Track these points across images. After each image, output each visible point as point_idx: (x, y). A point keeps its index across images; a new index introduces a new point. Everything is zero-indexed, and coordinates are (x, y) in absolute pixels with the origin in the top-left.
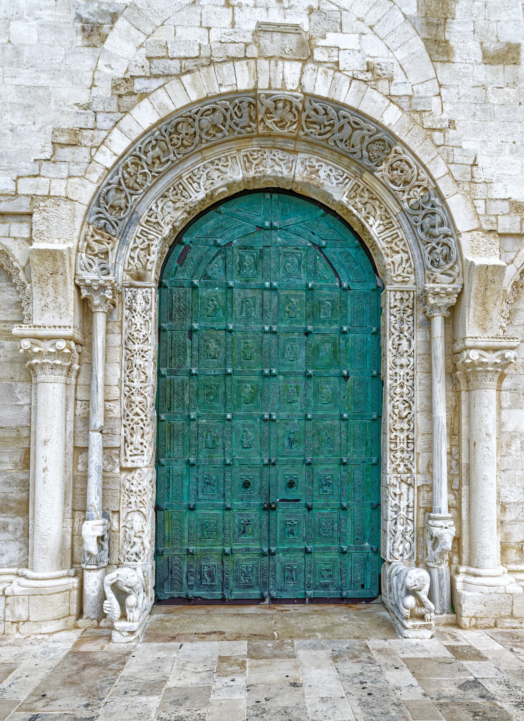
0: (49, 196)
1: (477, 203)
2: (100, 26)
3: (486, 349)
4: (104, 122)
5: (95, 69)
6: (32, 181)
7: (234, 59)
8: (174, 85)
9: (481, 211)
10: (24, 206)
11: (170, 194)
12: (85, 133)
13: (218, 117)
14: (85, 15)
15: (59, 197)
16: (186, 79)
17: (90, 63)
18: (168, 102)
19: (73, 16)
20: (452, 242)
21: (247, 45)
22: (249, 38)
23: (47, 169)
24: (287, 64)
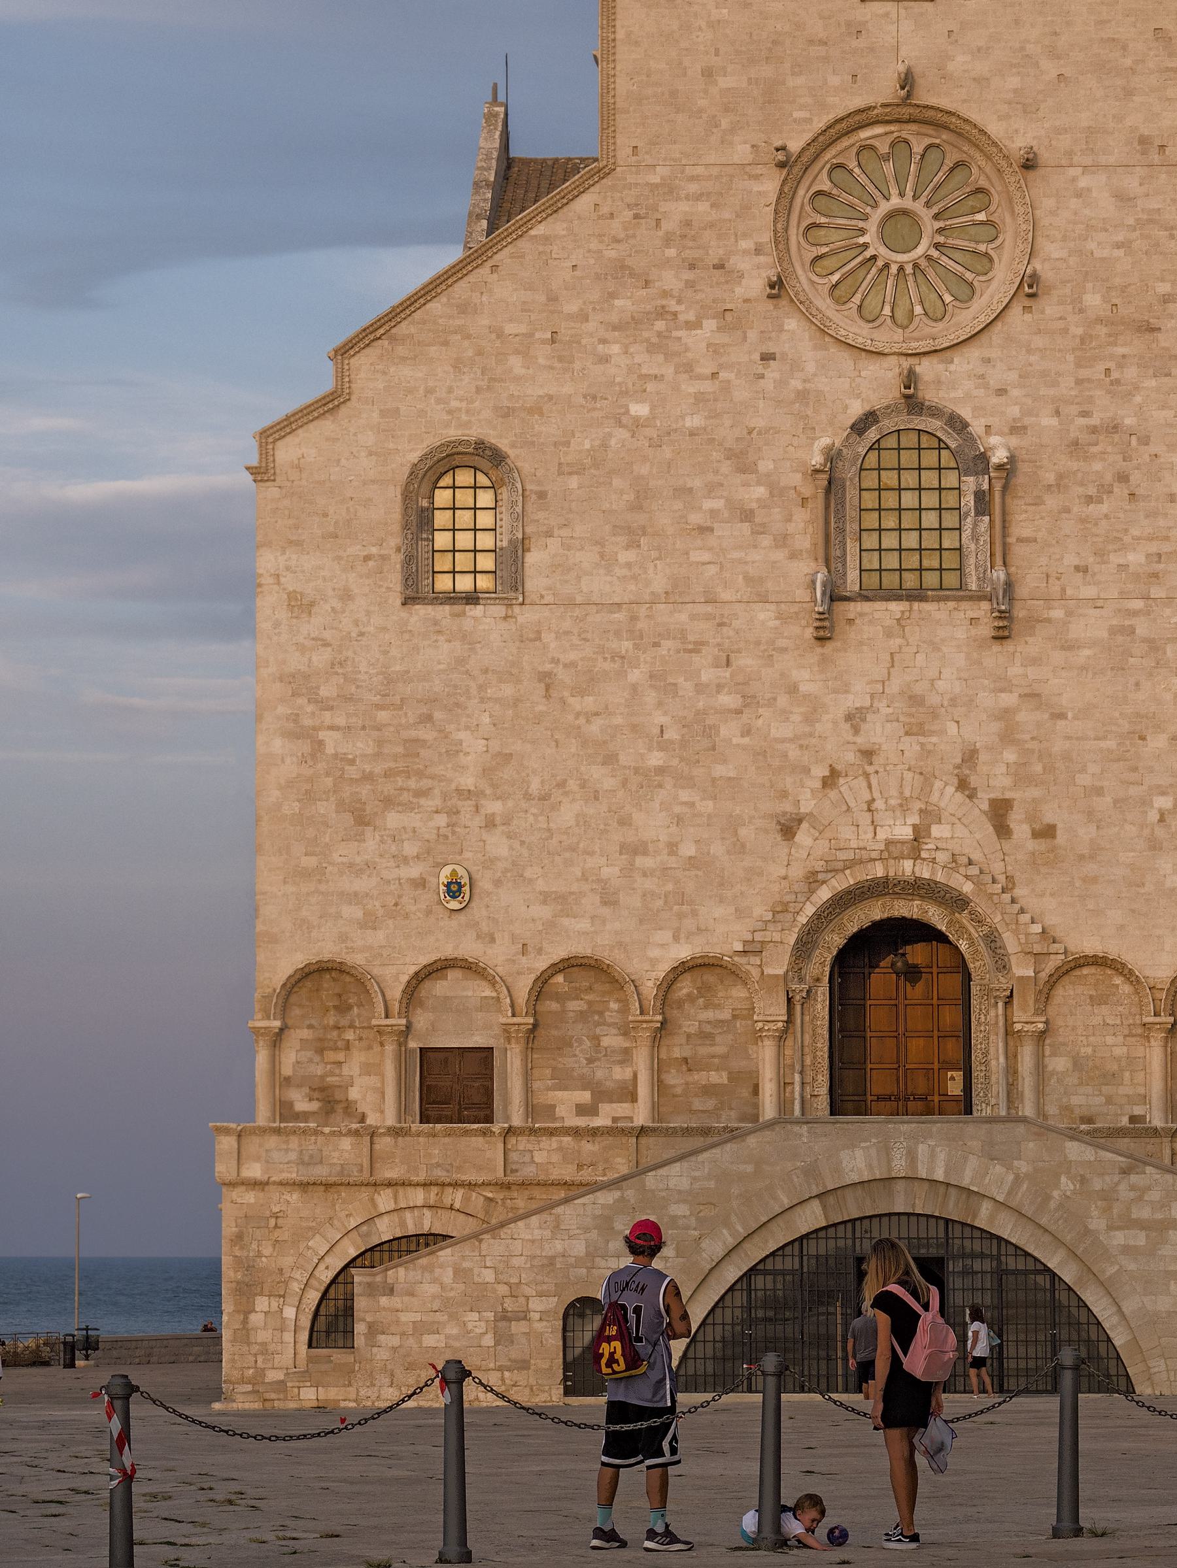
0: (771, 941)
1: (1020, 936)
2: (791, 828)
3: (1027, 1023)
4: (801, 898)
5: (790, 854)
6: (762, 933)
7: (875, 860)
8: (840, 876)
9: (1023, 941)
10: (758, 947)
11: (836, 929)
12: (791, 905)
13: (865, 889)
14: (783, 821)
15: (777, 942)
16: (848, 872)
17: (786, 850)
18: (837, 885)
19: (775, 822)
20: (1006, 959)
21: (882, 851)
22: (883, 848)
23: (771, 927)
24: (905, 861)
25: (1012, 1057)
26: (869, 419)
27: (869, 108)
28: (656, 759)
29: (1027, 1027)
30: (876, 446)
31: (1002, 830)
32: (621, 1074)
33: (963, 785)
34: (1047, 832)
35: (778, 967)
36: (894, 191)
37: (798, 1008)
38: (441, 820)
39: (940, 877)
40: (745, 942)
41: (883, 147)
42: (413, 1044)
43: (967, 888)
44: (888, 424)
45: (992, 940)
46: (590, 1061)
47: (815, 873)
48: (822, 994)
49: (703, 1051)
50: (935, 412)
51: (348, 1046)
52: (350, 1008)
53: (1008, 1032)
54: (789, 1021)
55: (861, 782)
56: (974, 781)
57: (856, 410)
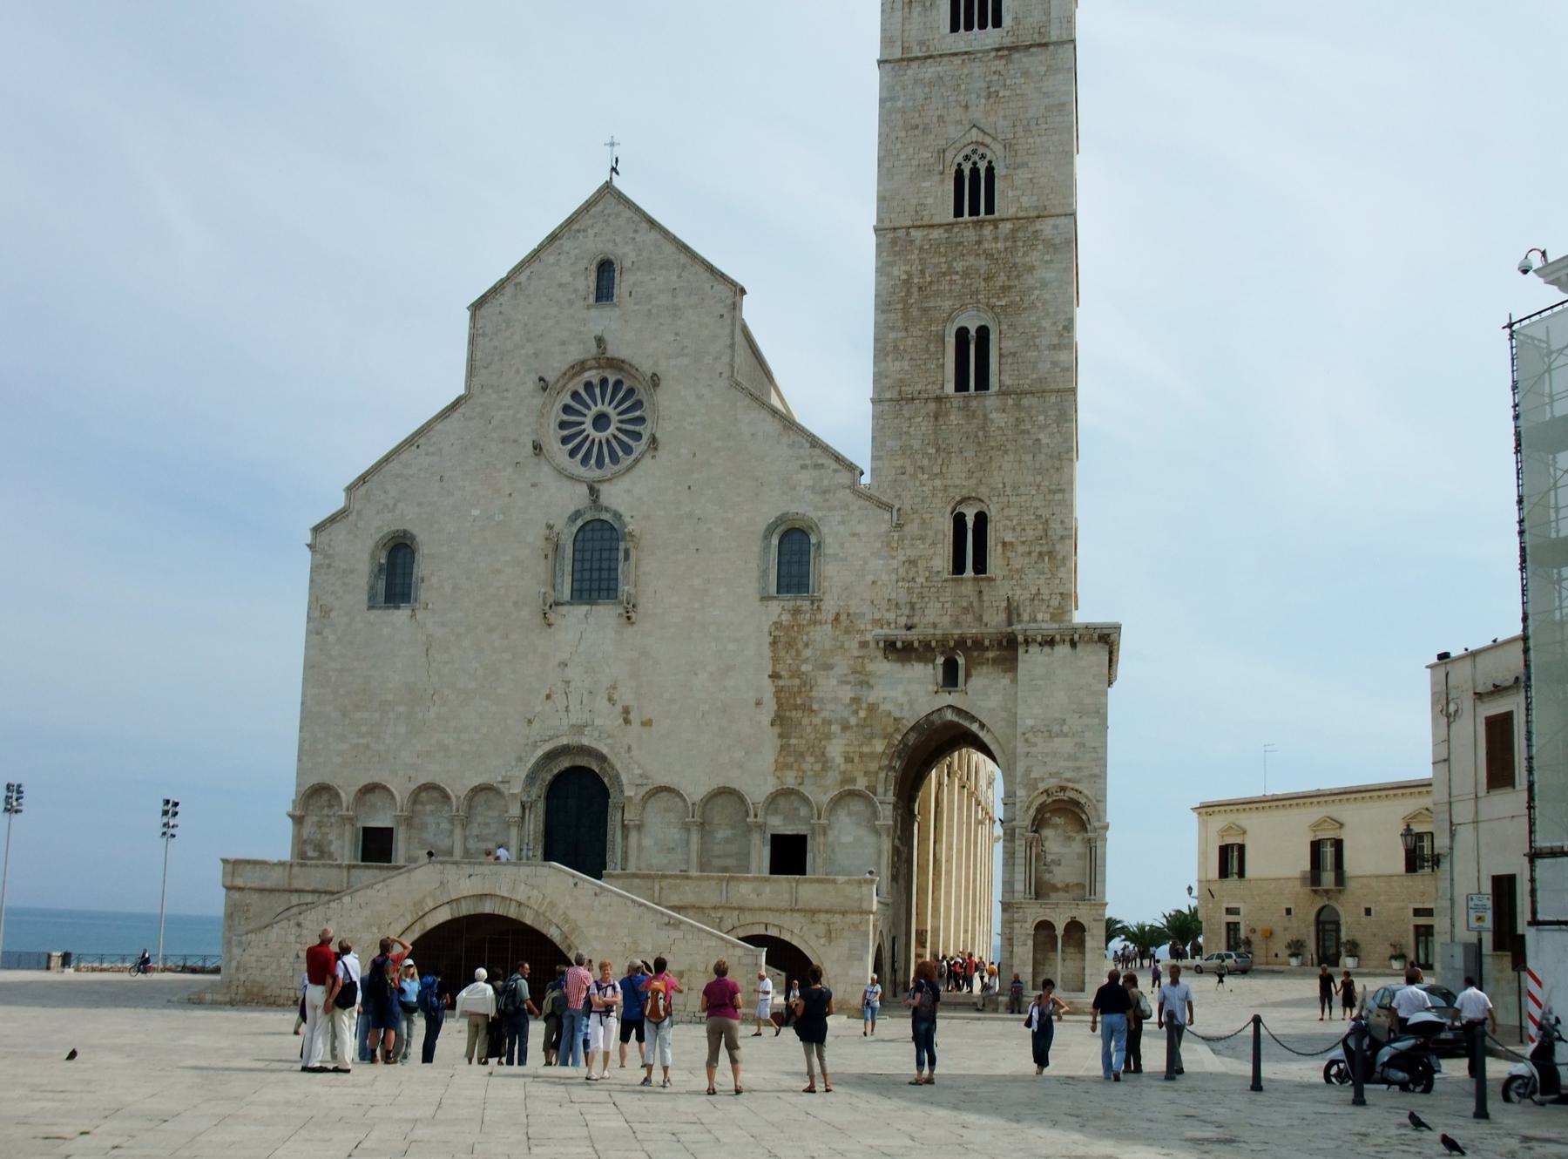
25: (625, 837)
26: (577, 515)
27: (587, 360)
28: (472, 685)
29: (632, 823)
30: (581, 529)
31: (627, 721)
32: (446, 843)
33: (610, 700)
34: (647, 723)
35: (517, 788)
36: (599, 402)
37: (527, 811)
38: (377, 716)
39: (594, 744)
40: (503, 777)
41: (596, 381)
42: (360, 825)
43: (605, 751)
44: (588, 517)
45: (617, 776)
46: (435, 835)
47: (536, 742)
48: (541, 806)
49: (486, 831)
50: (607, 510)
51: (332, 825)
52: (333, 806)
53: (624, 826)
54: (523, 817)
55: (565, 696)
56: (616, 697)
57: (572, 509)
